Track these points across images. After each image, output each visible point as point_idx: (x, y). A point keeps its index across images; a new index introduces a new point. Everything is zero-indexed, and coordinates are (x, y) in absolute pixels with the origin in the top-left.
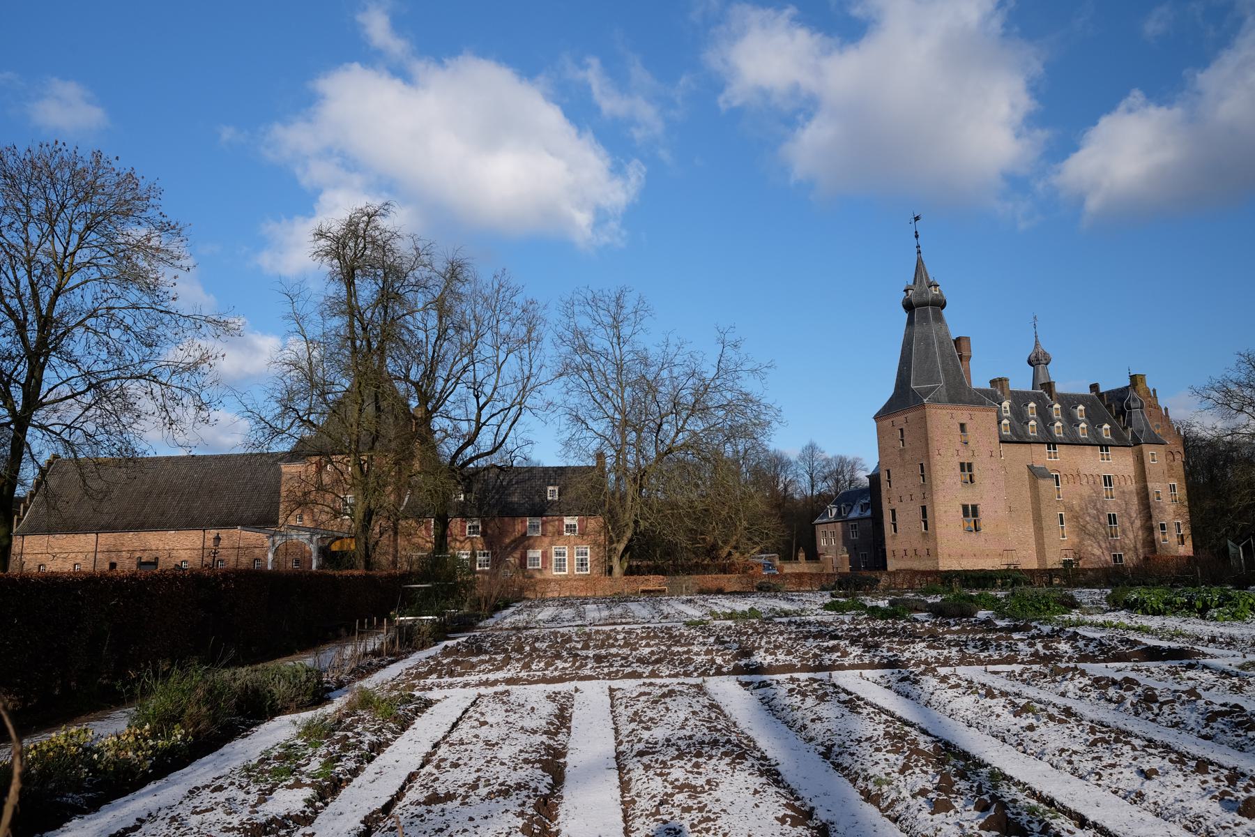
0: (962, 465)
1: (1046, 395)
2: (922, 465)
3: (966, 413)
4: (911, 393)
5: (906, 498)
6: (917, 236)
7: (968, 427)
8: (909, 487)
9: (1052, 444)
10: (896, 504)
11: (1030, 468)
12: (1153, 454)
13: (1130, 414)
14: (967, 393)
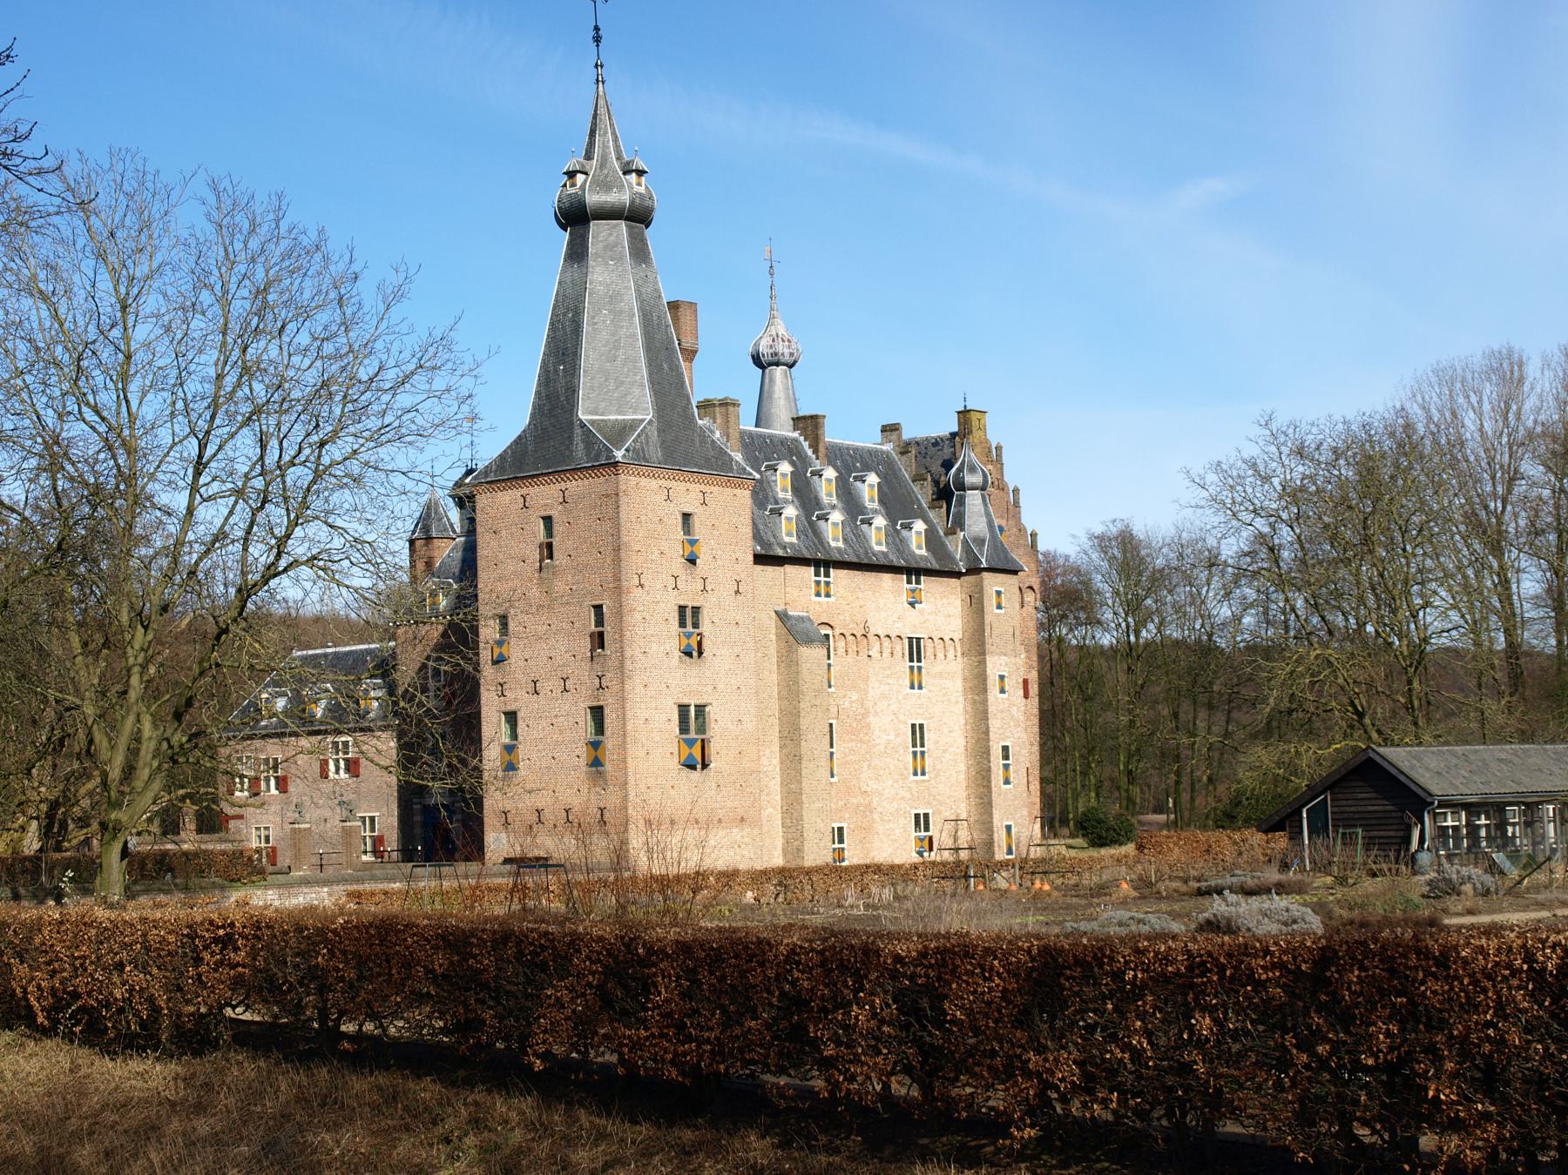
0: (682, 609)
1: (806, 445)
2: (598, 608)
3: (696, 488)
4: (578, 431)
5: (549, 685)
6: (597, 39)
7: (696, 522)
8: (558, 661)
9: (824, 564)
10: (518, 698)
11: (782, 616)
12: (999, 593)
13: (961, 501)
14: (697, 440)
